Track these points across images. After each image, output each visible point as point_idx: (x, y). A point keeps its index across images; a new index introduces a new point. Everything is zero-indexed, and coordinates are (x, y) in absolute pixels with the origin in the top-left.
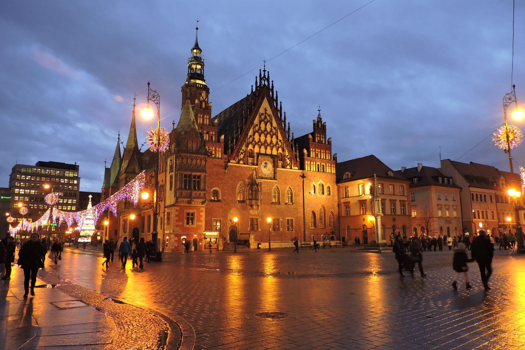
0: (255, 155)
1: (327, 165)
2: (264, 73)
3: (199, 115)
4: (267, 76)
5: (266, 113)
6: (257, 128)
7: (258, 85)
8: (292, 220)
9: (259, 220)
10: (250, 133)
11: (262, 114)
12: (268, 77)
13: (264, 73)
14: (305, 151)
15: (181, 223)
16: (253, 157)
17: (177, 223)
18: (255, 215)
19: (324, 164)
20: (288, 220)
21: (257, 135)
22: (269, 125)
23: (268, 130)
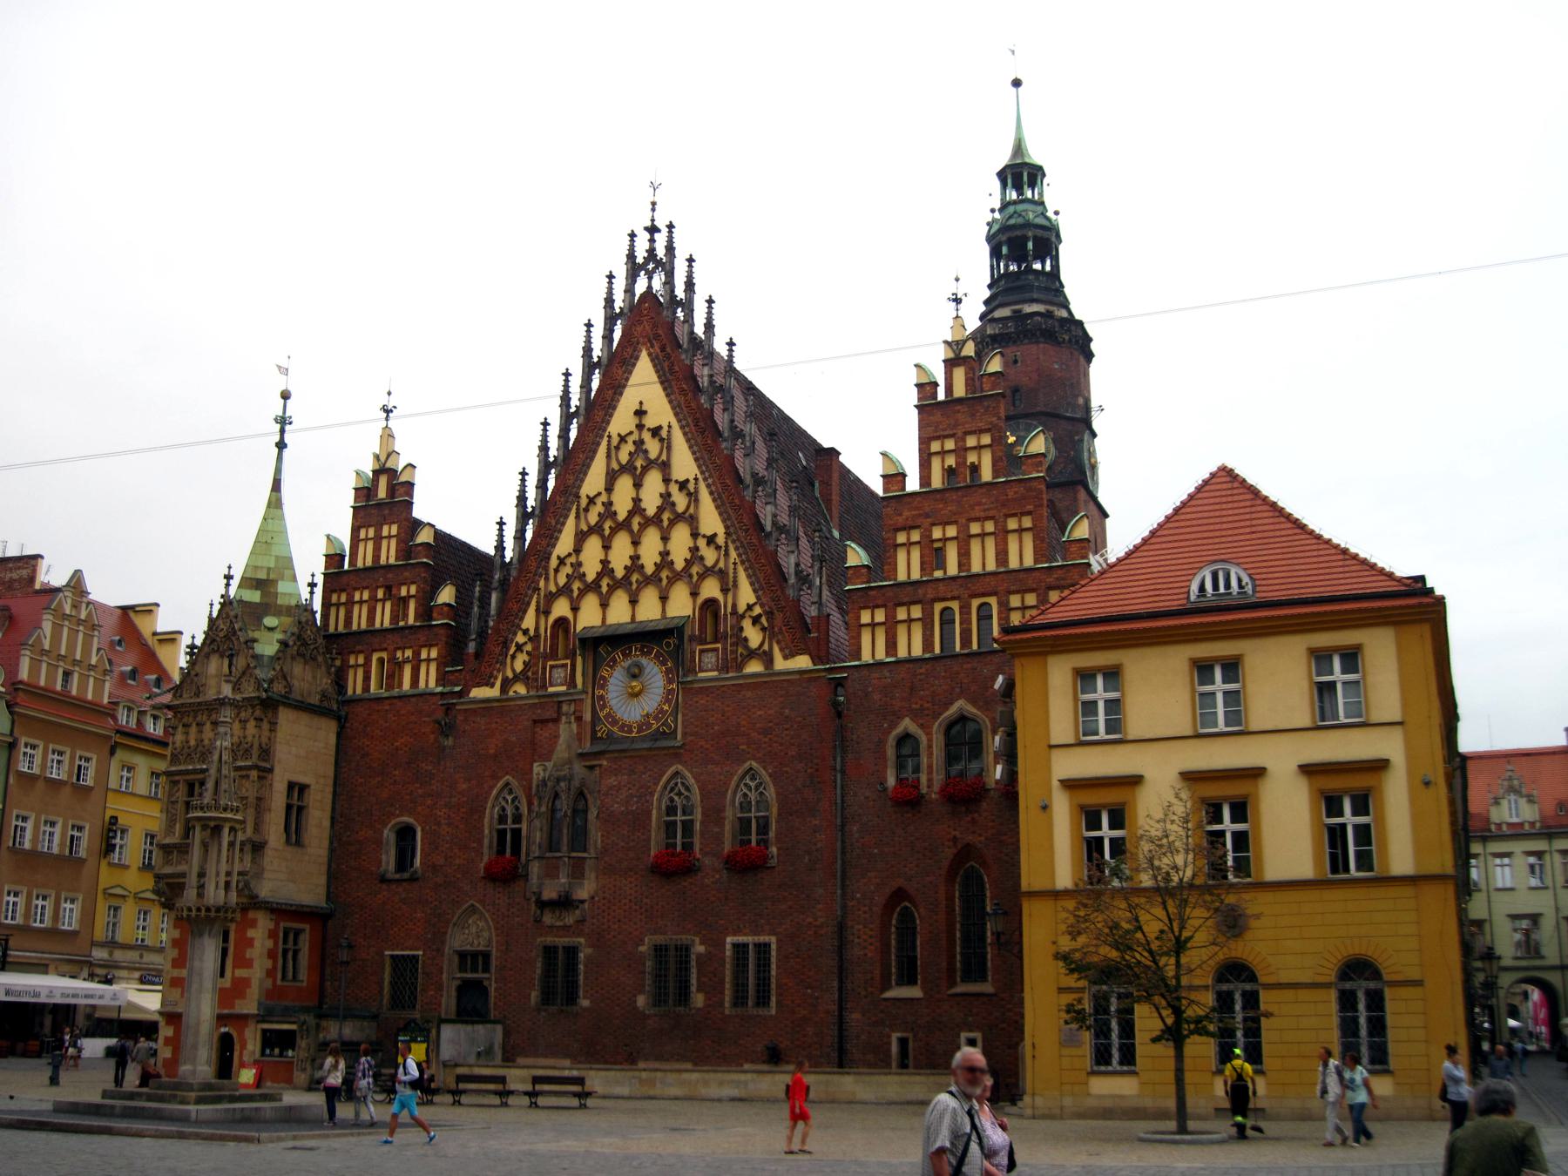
1: (1015, 601)
2: (652, 241)
3: (362, 534)
4: (661, 252)
7: (619, 304)
8: (763, 949)
10: (564, 544)
11: (623, 439)
12: (670, 249)
13: (652, 241)
14: (857, 556)
18: (566, 928)
19: (993, 601)
20: (740, 949)
21: (593, 546)
23: (651, 504)
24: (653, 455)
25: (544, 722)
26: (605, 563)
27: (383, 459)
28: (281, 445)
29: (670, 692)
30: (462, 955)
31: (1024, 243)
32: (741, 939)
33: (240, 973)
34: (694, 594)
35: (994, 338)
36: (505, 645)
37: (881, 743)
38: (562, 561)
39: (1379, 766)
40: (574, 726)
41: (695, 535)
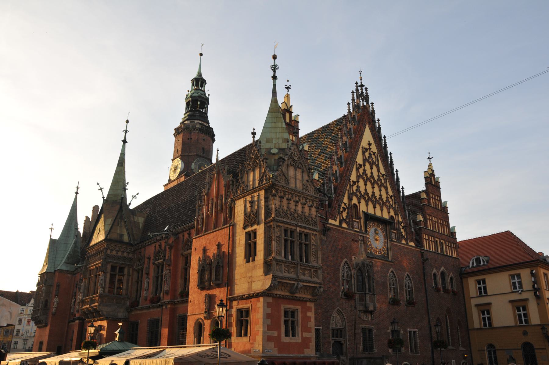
0: (362, 215)
5: (370, 149)
6: (361, 171)
8: (414, 332)
9: (375, 331)
11: (366, 150)
12: (367, 96)
13: (362, 89)
14: (420, 218)
15: (276, 334)
16: (359, 218)
17: (271, 333)
22: (375, 168)
24: (374, 160)
25: (354, 240)
26: (366, 190)
27: (289, 107)
28: (274, 78)
29: (385, 242)
30: (333, 329)
31: (197, 104)
32: (411, 329)
33: (305, 335)
34: (389, 212)
35: (200, 130)
36: (340, 206)
37: (431, 274)
38: (354, 183)
39: (527, 300)
40: (363, 245)
41: (387, 193)
